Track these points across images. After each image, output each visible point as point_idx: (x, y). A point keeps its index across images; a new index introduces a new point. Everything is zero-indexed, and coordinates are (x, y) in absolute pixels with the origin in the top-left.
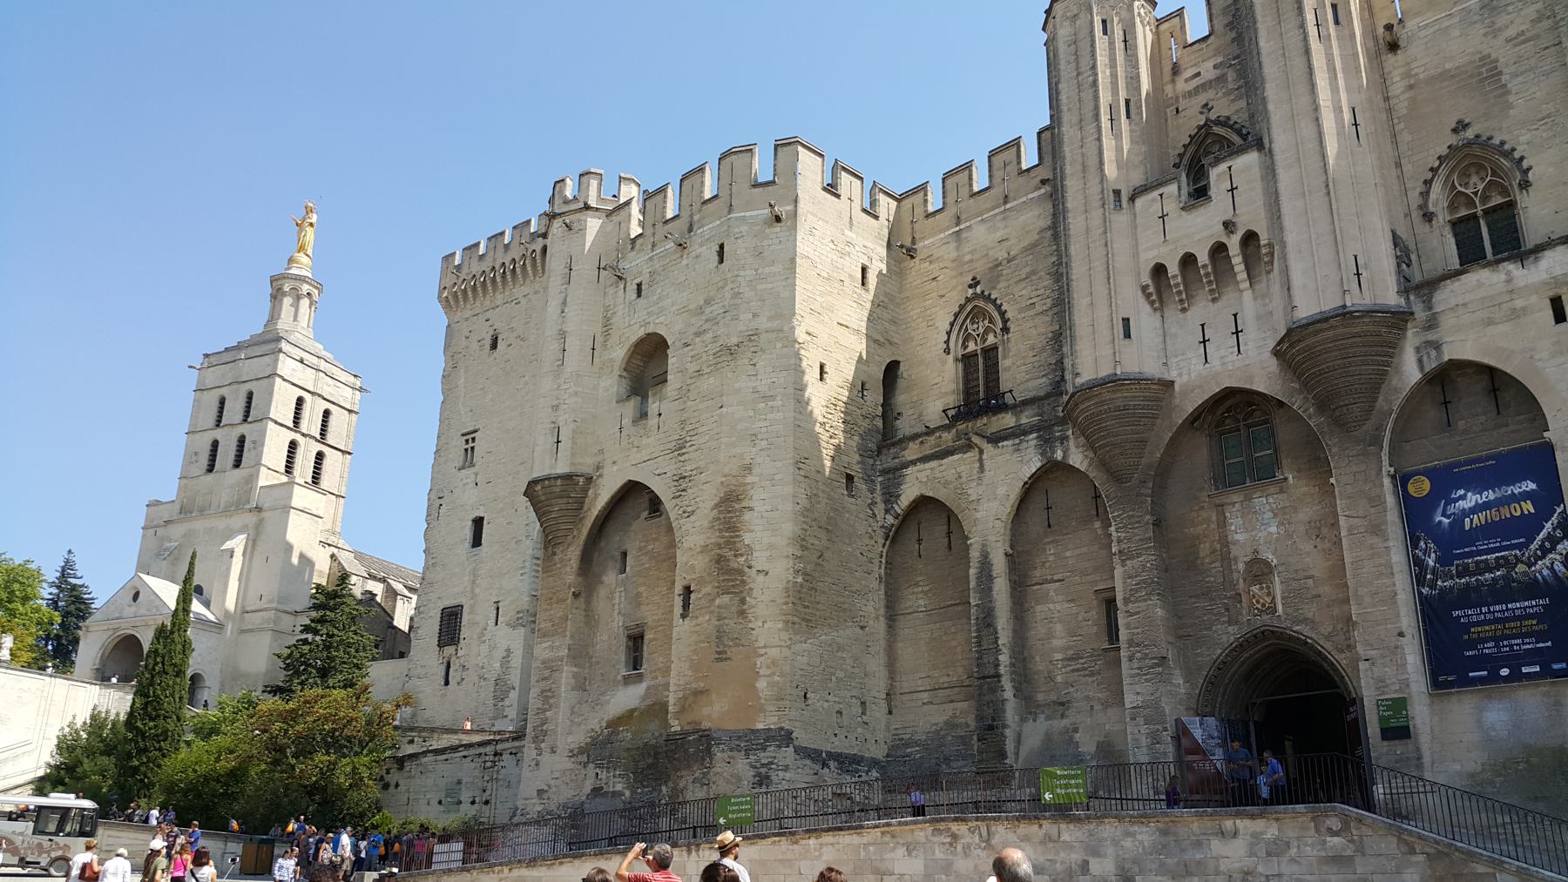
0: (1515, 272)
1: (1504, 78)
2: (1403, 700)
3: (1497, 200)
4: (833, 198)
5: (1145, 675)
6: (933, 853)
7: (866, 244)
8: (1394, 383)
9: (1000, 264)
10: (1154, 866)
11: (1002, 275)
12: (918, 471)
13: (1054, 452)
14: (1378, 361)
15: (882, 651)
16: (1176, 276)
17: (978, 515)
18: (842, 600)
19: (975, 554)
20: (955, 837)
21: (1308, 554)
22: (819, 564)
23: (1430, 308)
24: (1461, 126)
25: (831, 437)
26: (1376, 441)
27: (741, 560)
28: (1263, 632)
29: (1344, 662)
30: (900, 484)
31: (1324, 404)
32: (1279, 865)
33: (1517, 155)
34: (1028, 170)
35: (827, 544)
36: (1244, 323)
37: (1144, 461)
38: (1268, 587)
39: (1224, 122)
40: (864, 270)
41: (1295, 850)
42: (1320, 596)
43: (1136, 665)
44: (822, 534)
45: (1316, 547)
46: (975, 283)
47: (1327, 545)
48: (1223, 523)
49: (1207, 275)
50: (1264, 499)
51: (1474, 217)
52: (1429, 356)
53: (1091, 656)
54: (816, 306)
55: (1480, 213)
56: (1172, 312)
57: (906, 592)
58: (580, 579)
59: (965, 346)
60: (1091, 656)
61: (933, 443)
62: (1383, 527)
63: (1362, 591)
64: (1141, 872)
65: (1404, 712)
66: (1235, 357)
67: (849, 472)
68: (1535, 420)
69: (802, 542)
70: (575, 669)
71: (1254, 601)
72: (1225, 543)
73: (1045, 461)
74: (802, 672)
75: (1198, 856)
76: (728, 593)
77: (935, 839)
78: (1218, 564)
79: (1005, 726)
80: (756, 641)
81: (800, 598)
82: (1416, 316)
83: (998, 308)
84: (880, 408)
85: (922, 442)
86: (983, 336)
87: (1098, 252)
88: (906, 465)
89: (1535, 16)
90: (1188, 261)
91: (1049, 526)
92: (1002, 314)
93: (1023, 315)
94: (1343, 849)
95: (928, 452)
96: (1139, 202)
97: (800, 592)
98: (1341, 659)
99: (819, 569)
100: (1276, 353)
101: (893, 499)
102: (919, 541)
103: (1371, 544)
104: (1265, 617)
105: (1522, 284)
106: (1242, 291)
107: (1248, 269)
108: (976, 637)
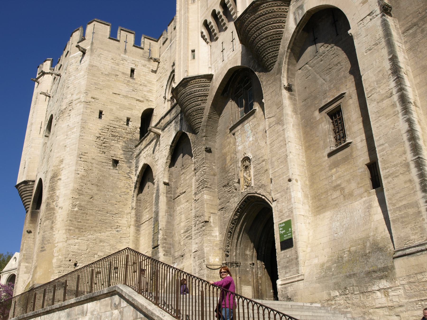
7: (134, 59)
8: (285, 36)
14: (275, 26)
22: (90, 202)
25: (104, 143)
26: (279, 71)
27: (55, 203)
40: (132, 71)
43: (197, 228)
44: (95, 188)
50: (248, 124)
57: (144, 213)
58: (31, 225)
65: (290, 229)
67: (114, 158)
69: (79, 192)
70: (27, 264)
76: (48, 220)
80: (55, 240)
81: (76, 218)
84: (139, 130)
85: (146, 140)
99: (90, 204)
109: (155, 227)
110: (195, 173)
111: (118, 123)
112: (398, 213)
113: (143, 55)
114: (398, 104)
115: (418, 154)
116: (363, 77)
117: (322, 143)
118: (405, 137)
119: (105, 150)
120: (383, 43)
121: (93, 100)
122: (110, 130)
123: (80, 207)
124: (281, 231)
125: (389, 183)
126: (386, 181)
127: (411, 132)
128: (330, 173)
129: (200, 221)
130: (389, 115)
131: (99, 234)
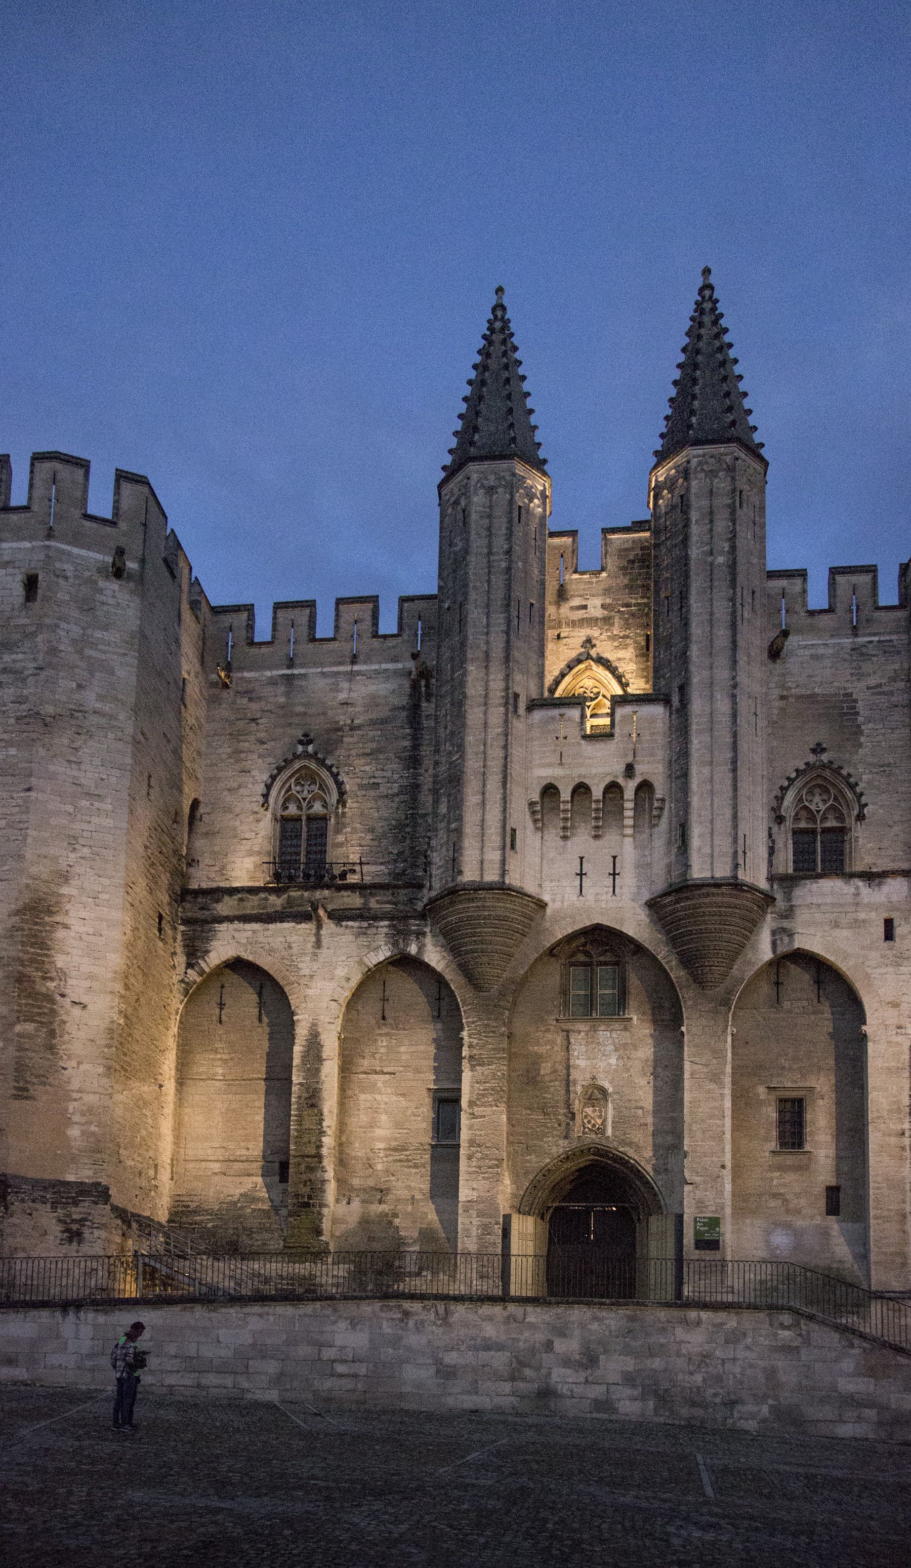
0: (863, 888)
6: (381, 1328)
16: (567, 802)
20: (407, 1314)
23: (789, 900)
49: (597, 810)
52: (782, 939)
56: (553, 835)
77: (383, 1315)
80: (69, 1083)
87: (496, 753)
90: (581, 790)
96: (538, 715)
97: (121, 1036)
106: (624, 836)
107: (634, 817)
123: (126, 1017)
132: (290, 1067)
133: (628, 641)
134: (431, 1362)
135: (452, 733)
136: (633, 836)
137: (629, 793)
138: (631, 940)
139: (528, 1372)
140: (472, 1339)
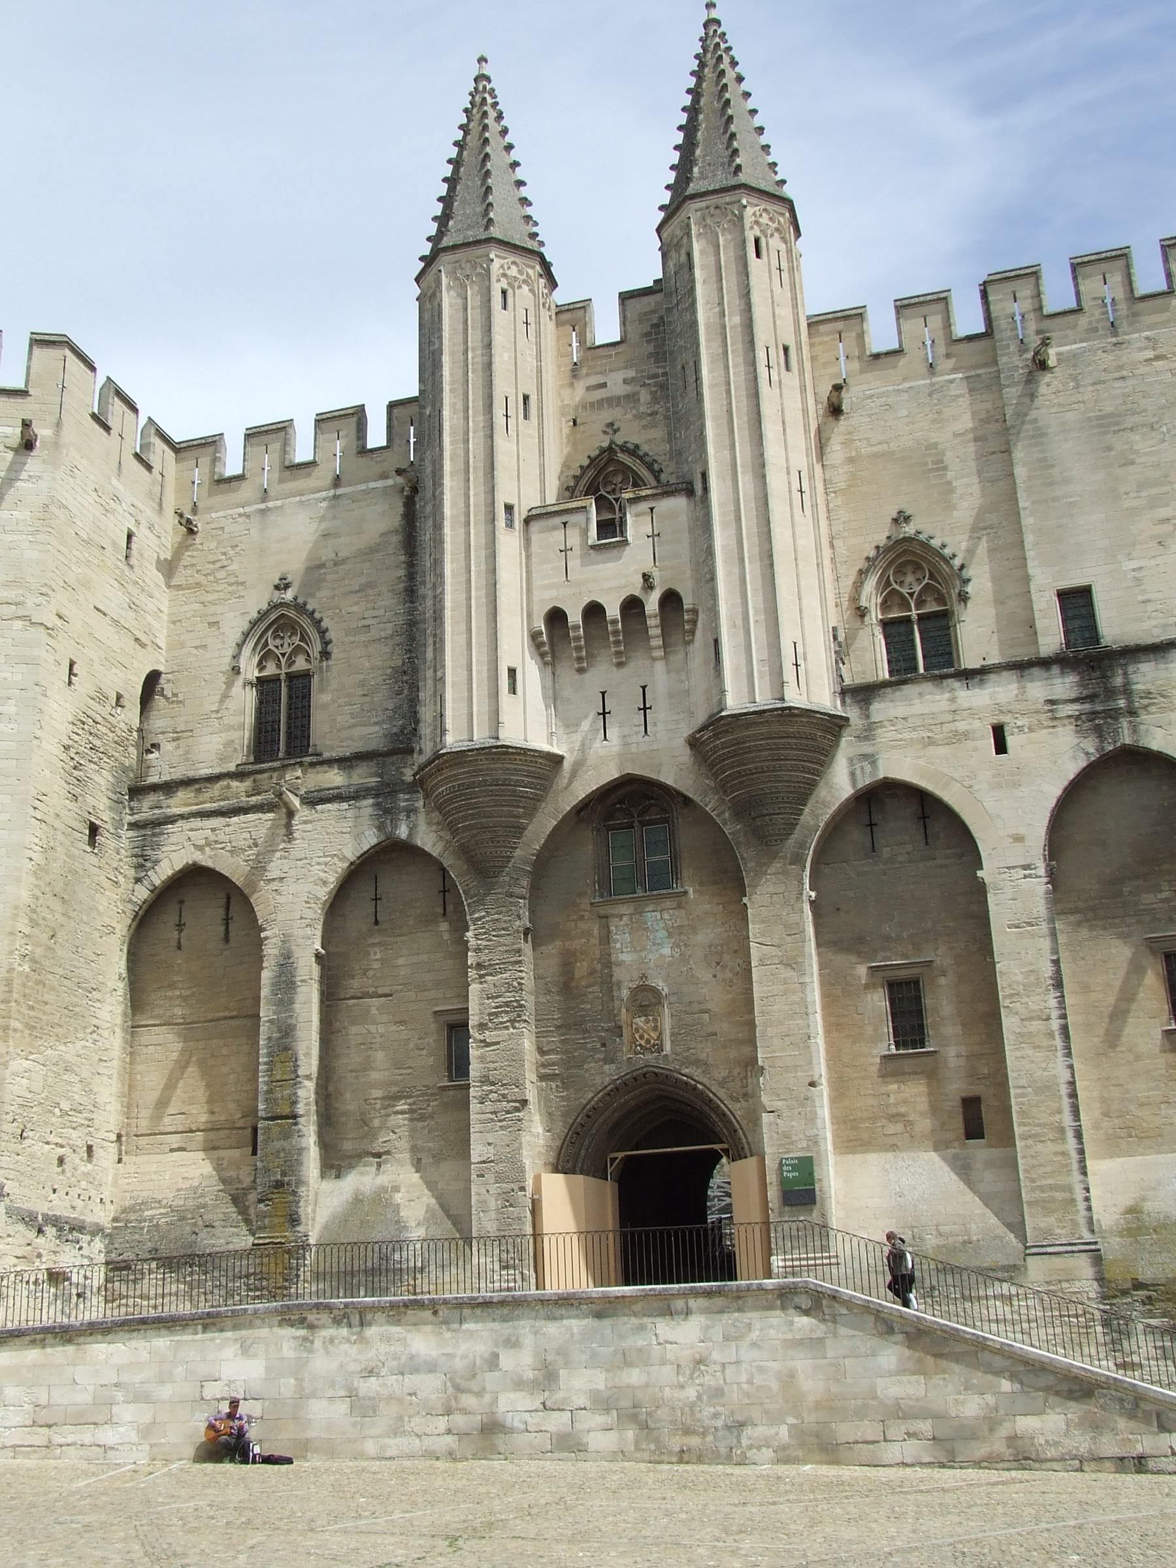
1: (950, 475)
2: (811, 1157)
3: (932, 607)
4: (102, 431)
5: (500, 1121)
9: (322, 566)
10: (584, 1357)
11: (325, 580)
12: (191, 830)
13: (396, 827)
14: (808, 768)
15: (115, 1076)
17: (281, 899)
18: (74, 999)
19: (271, 950)
21: (706, 983)
22: (50, 949)
23: (868, 717)
24: (902, 518)
26: (798, 860)
28: (644, 1075)
29: (738, 1114)
30: (157, 846)
31: (744, 809)
32: (737, 1351)
33: (957, 563)
34: (372, 451)
35: (62, 920)
36: (654, 699)
37: (518, 852)
38: (655, 1020)
39: (633, 451)
40: (130, 536)
41: (757, 1333)
42: (715, 1034)
43: (489, 1109)
44: (57, 905)
45: (715, 976)
46: (283, 585)
47: (728, 975)
48: (606, 939)
49: (616, 632)
50: (658, 915)
51: (908, 620)
52: (862, 768)
53: (422, 1095)
54: (71, 579)
55: (915, 617)
59: (265, 667)
60: (422, 1095)
61: (217, 793)
62: (800, 960)
63: (771, 1032)
64: (567, 1364)
66: (640, 739)
68: (963, 855)
71: (637, 1036)
72: (607, 963)
73: (383, 838)
74: (20, 1101)
75: (641, 1343)
78: (596, 988)
79: (299, 1182)
81: (25, 996)
82: (852, 722)
83: (317, 623)
84: (135, 734)
85: (199, 790)
86: (290, 657)
88: (171, 820)
89: (984, 415)
90: (594, 611)
91: (376, 922)
92: (323, 632)
93: (352, 639)
94: (812, 1331)
95: (208, 806)
97: (24, 985)
98: (737, 1109)
100: (693, 743)
101: (149, 864)
102: (180, 926)
103: (785, 979)
104: (649, 1056)
105: (966, 705)
106: (654, 659)
107: (664, 634)
108: (265, 1064)
109: (279, 1065)
110: (481, 976)
111: (98, 708)
112: (1038, 1195)
113: (150, 490)
114: (1057, 1036)
115: (1079, 1120)
116: (998, 966)
117: (869, 1030)
118: (1064, 1090)
119: (77, 791)
120: (1044, 927)
121: (59, 622)
122: (86, 727)
123: (34, 961)
124: (789, 1171)
125: (1027, 1147)
126: (1023, 1143)
127: (1072, 1083)
128: (884, 1089)
129: (504, 1096)
130: (1039, 1047)
131: (63, 1048)
132: (257, 999)
133: (659, 417)
134: (343, 1393)
135: (435, 560)
136: (665, 657)
137: (652, 604)
138: (679, 794)
139: (468, 1400)
140: (396, 1357)
